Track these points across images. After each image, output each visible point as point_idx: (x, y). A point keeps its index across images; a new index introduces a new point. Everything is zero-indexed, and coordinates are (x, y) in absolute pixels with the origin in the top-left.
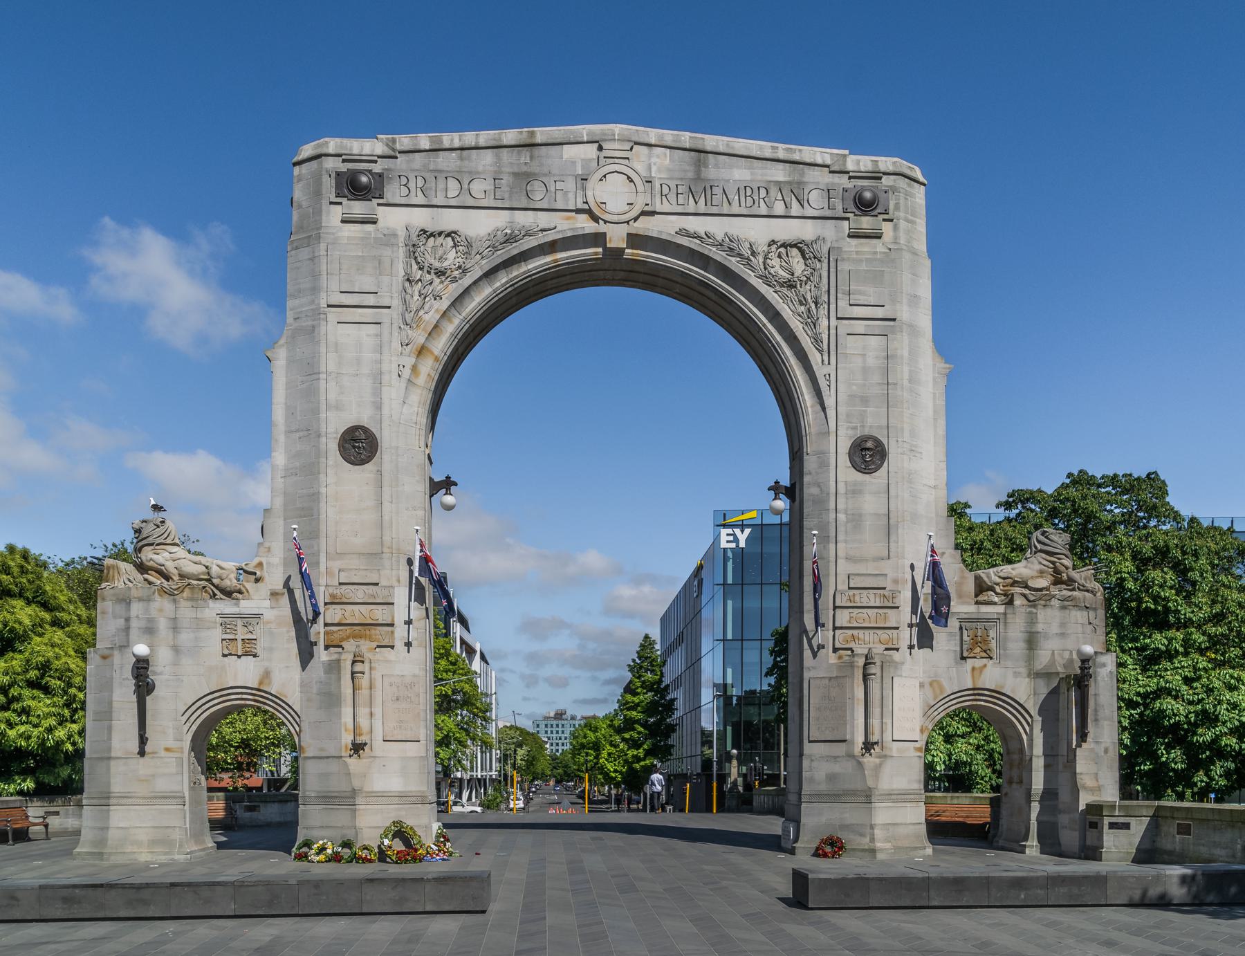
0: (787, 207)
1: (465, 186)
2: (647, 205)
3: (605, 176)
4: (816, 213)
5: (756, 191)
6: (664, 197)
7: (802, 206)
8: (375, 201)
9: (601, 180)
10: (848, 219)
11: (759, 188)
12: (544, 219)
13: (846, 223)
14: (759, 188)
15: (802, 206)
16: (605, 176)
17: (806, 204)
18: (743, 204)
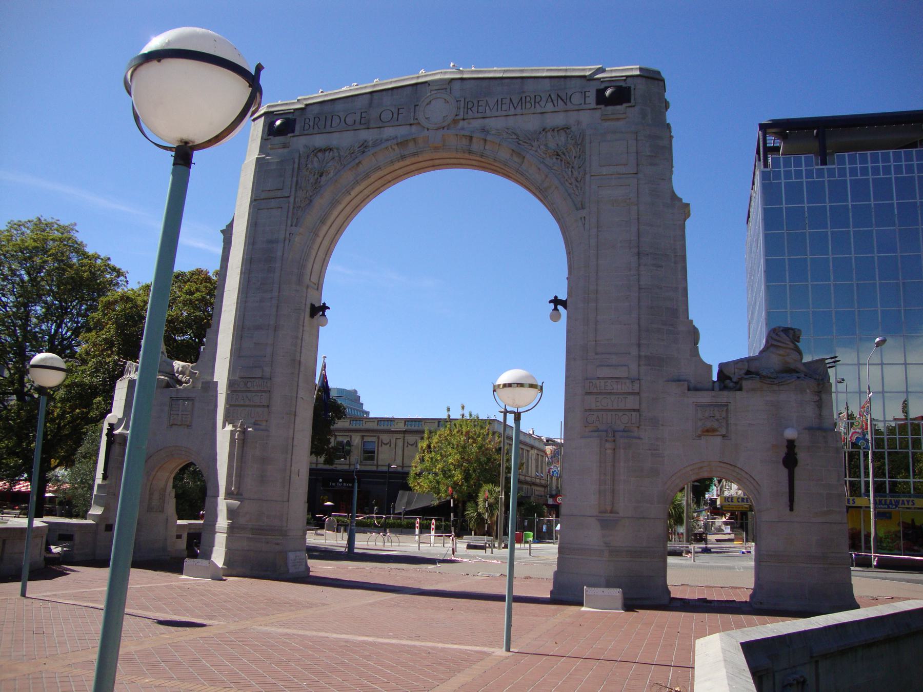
0: (554, 106)
1: (343, 119)
2: (456, 115)
3: (430, 101)
4: (577, 108)
5: (533, 97)
6: (469, 110)
7: (566, 105)
8: (290, 135)
9: (427, 104)
10: (600, 108)
11: (535, 96)
14: (535, 96)
15: (566, 105)
16: (430, 101)
17: (568, 103)
18: (524, 107)
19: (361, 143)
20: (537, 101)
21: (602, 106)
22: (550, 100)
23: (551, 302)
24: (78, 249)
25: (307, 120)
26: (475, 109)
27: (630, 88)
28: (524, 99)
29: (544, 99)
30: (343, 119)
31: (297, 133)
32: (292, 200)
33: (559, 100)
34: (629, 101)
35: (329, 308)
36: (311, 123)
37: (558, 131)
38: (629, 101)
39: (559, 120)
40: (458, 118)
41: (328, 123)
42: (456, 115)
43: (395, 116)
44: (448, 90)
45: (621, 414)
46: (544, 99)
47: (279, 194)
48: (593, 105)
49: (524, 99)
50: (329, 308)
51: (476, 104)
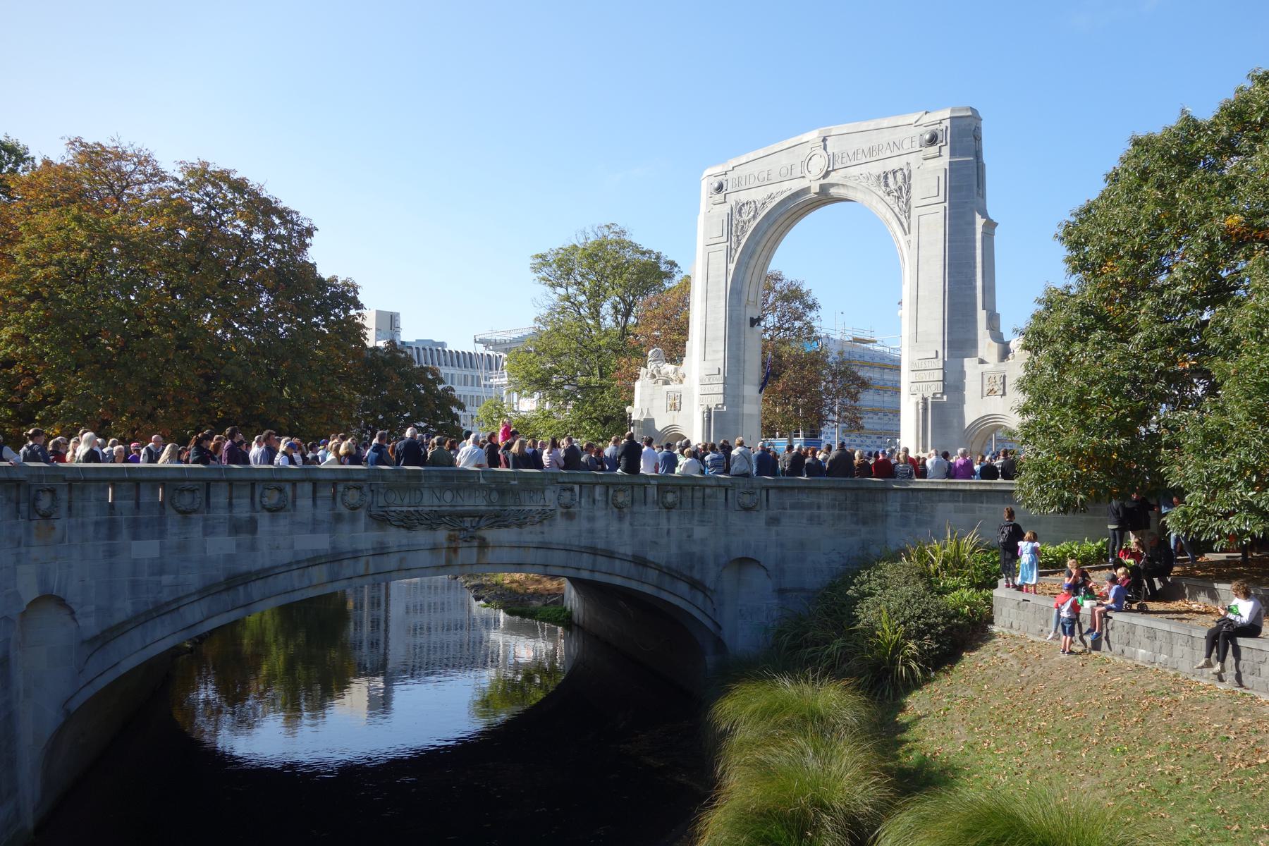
12: (786, 185)
13: (921, 155)
17: (901, 148)
24: (636, 249)
26: (840, 161)
27: (942, 130)
29: (885, 147)
32: (728, 244)
33: (895, 147)
37: (894, 173)
38: (942, 142)
40: (829, 169)
41: (748, 180)
42: (828, 167)
46: (885, 147)
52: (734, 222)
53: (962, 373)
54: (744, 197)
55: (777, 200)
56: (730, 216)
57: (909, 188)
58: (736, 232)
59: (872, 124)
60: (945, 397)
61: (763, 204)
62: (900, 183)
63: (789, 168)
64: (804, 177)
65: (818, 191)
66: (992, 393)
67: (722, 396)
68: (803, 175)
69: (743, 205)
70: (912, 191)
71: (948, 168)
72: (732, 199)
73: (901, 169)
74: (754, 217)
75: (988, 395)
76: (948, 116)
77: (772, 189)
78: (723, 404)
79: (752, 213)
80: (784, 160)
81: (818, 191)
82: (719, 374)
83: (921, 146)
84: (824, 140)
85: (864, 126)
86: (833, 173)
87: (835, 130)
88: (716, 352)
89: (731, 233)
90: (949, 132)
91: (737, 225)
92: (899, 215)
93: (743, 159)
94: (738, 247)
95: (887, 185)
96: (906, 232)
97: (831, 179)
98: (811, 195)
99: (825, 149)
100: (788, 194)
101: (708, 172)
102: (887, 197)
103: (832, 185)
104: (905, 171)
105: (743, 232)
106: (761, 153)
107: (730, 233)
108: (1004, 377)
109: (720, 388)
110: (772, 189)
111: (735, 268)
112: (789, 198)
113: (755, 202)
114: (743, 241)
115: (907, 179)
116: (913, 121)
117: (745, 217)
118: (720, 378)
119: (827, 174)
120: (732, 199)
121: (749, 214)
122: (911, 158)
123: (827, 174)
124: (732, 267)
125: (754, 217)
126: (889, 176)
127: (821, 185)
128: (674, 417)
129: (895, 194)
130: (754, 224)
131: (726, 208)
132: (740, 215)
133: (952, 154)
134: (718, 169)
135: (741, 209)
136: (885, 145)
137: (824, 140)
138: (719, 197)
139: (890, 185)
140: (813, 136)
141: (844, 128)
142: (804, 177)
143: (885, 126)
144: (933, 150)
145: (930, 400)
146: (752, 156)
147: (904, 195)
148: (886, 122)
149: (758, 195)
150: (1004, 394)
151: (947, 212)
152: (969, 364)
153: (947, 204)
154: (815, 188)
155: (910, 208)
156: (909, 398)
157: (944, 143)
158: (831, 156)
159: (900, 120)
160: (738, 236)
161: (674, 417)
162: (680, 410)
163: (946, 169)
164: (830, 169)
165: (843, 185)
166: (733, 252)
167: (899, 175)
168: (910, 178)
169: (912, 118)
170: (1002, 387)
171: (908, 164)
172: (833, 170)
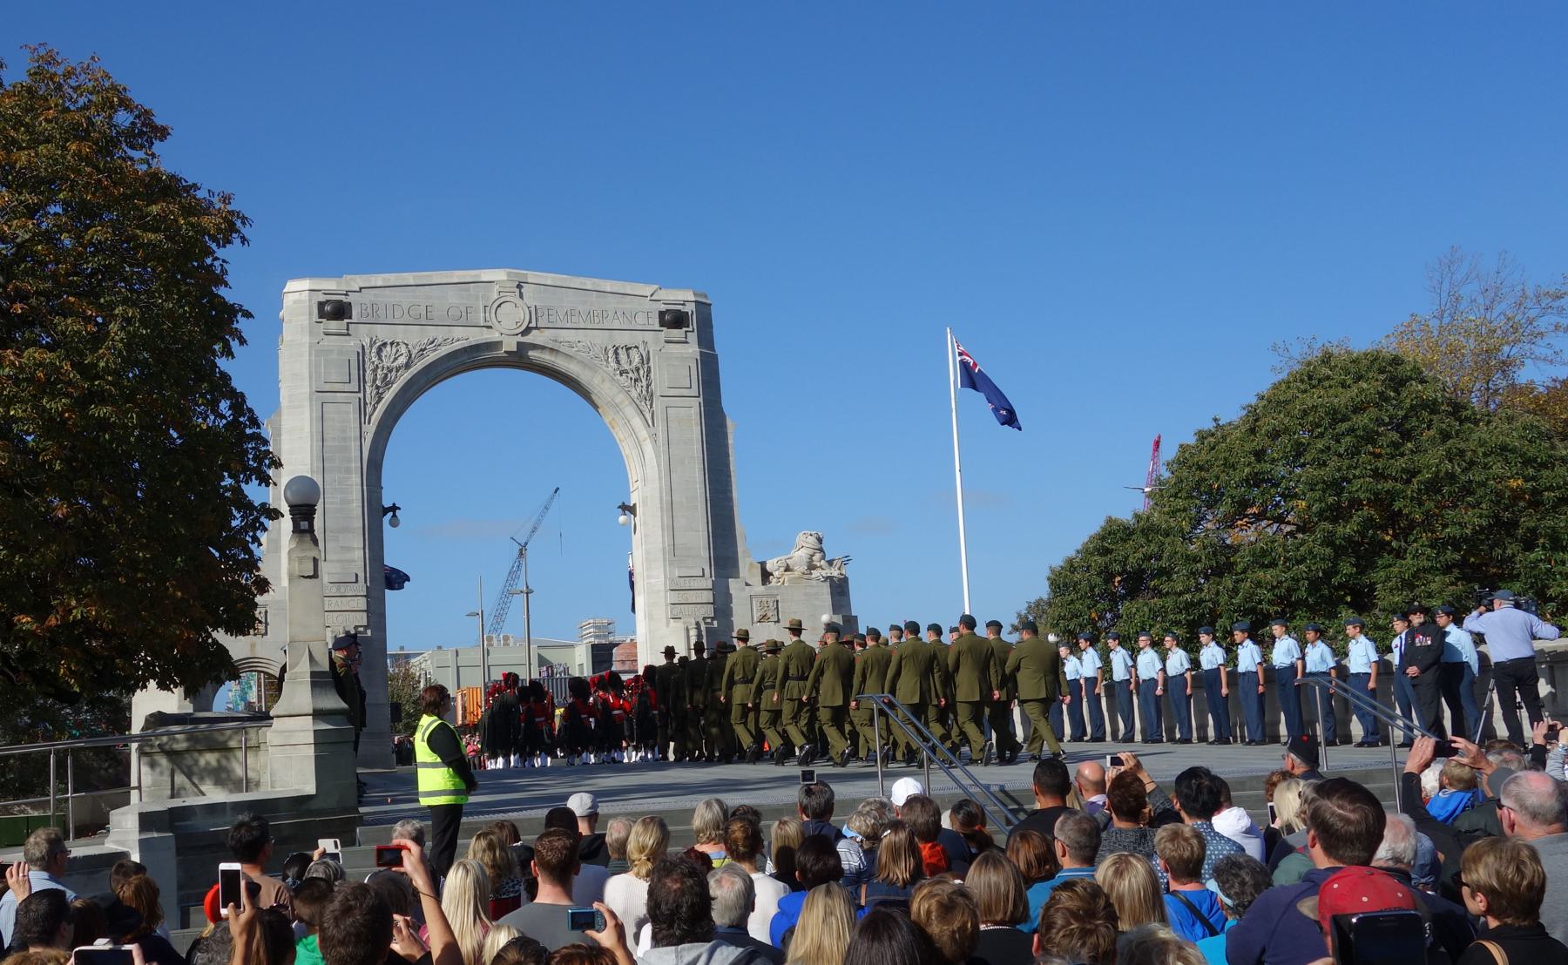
12: (458, 332)
19: (431, 339)
20: (604, 316)
21: (664, 329)
22: (616, 317)
23: (620, 507)
25: (363, 306)
27: (687, 313)
28: (592, 313)
30: (406, 312)
31: (355, 318)
32: (361, 395)
34: (688, 327)
35: (399, 509)
36: (369, 310)
38: (688, 327)
39: (623, 339)
40: (531, 325)
42: (530, 322)
43: (464, 314)
44: (517, 293)
45: (699, 606)
47: (347, 387)
48: (657, 327)
49: (592, 313)
50: (399, 509)
51: (546, 313)
52: (369, 368)
53: (728, 597)
54: (383, 333)
55: (444, 351)
56: (362, 355)
57: (649, 371)
58: (374, 380)
59: (589, 283)
60: (715, 623)
61: (422, 350)
62: (636, 360)
63: (464, 310)
64: (490, 327)
65: (515, 349)
66: (763, 618)
67: (365, 614)
68: (490, 324)
69: (385, 344)
70: (652, 375)
71: (699, 358)
72: (363, 335)
73: (636, 347)
74: (408, 366)
75: (759, 622)
76: (694, 299)
77: (439, 334)
78: (366, 627)
79: (402, 360)
80: (453, 297)
81: (515, 349)
82: (357, 582)
83: (661, 326)
84: (519, 286)
85: (576, 282)
86: (534, 332)
87: (532, 276)
88: (349, 549)
89: (365, 382)
90: (694, 317)
91: (375, 370)
92: (637, 402)
93: (378, 280)
94: (378, 402)
95: (618, 362)
96: (650, 423)
97: (533, 338)
98: (501, 353)
99: (521, 296)
100: (464, 344)
101: (292, 286)
102: (618, 377)
103: (534, 347)
104: (641, 349)
105: (388, 384)
106: (409, 278)
107: (362, 380)
108: (777, 601)
109: (361, 603)
110: (439, 334)
111: (376, 433)
112: (465, 350)
113: (407, 345)
114: (389, 396)
115: (645, 360)
116: (649, 294)
117: (386, 363)
118: (361, 588)
119: (527, 331)
120: (363, 335)
121: (396, 359)
122: (648, 336)
123: (527, 331)
124: (370, 430)
125: (408, 366)
126: (620, 351)
127: (519, 344)
128: (253, 646)
129: (631, 375)
130: (407, 376)
131: (352, 344)
132: (380, 358)
133: (700, 344)
134: (330, 285)
135: (380, 350)
136: (611, 313)
137: (519, 286)
138: (334, 325)
139: (622, 362)
140: (499, 275)
141: (549, 278)
142: (490, 327)
143: (609, 290)
144: (677, 334)
145: (703, 627)
146: (392, 278)
147: (644, 380)
148: (608, 285)
149: (414, 337)
150: (778, 621)
151: (702, 408)
152: (734, 585)
153: (701, 399)
154: (510, 345)
155: (652, 395)
156: (668, 624)
157: (691, 329)
158: (533, 310)
159: (629, 288)
160: (378, 387)
161: (253, 646)
162: (266, 634)
163: (697, 360)
164: (533, 324)
165: (552, 350)
166: (369, 409)
167: (633, 352)
168: (648, 359)
169: (647, 290)
170: (776, 613)
171: (645, 343)
172: (536, 328)
